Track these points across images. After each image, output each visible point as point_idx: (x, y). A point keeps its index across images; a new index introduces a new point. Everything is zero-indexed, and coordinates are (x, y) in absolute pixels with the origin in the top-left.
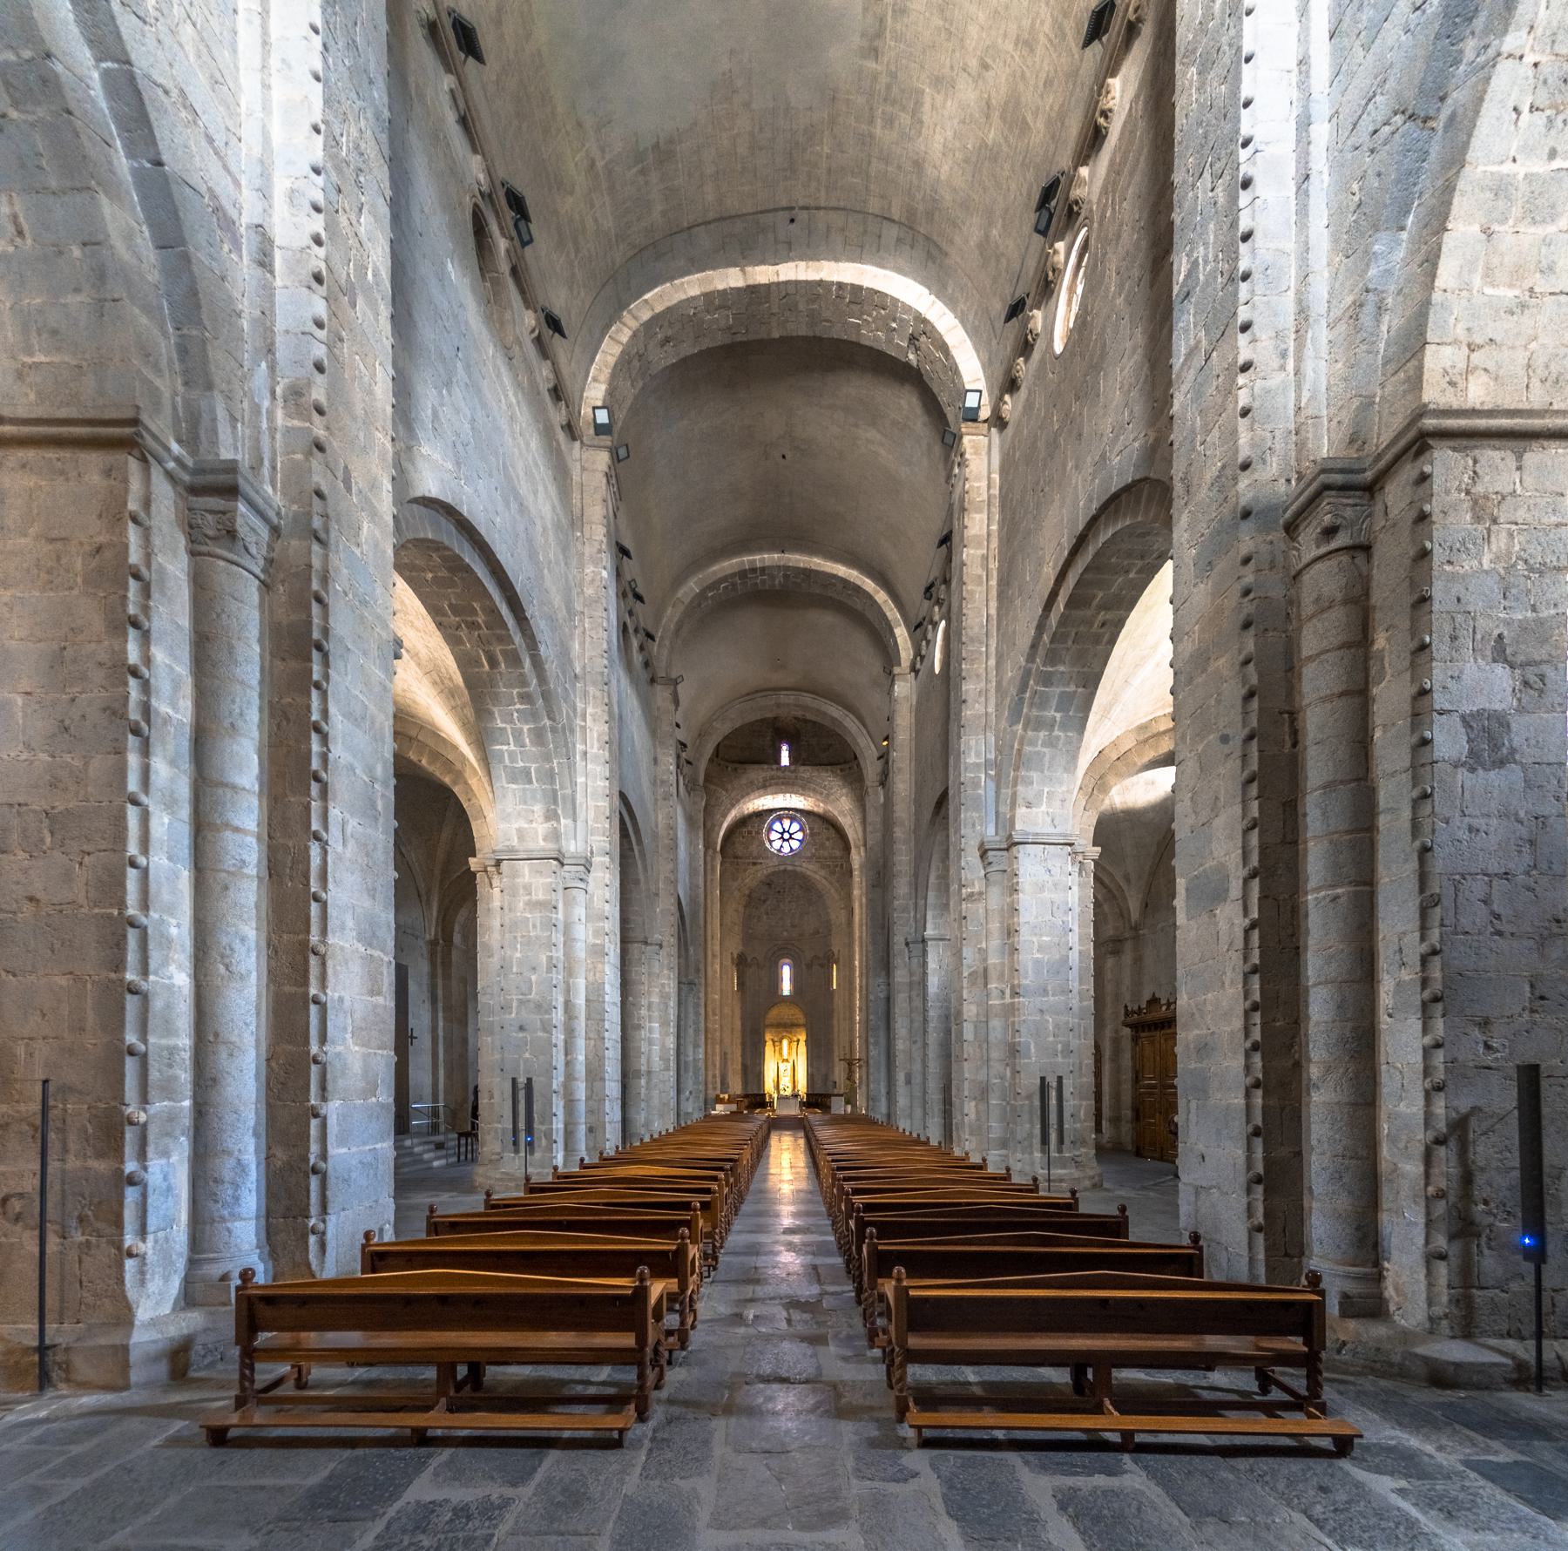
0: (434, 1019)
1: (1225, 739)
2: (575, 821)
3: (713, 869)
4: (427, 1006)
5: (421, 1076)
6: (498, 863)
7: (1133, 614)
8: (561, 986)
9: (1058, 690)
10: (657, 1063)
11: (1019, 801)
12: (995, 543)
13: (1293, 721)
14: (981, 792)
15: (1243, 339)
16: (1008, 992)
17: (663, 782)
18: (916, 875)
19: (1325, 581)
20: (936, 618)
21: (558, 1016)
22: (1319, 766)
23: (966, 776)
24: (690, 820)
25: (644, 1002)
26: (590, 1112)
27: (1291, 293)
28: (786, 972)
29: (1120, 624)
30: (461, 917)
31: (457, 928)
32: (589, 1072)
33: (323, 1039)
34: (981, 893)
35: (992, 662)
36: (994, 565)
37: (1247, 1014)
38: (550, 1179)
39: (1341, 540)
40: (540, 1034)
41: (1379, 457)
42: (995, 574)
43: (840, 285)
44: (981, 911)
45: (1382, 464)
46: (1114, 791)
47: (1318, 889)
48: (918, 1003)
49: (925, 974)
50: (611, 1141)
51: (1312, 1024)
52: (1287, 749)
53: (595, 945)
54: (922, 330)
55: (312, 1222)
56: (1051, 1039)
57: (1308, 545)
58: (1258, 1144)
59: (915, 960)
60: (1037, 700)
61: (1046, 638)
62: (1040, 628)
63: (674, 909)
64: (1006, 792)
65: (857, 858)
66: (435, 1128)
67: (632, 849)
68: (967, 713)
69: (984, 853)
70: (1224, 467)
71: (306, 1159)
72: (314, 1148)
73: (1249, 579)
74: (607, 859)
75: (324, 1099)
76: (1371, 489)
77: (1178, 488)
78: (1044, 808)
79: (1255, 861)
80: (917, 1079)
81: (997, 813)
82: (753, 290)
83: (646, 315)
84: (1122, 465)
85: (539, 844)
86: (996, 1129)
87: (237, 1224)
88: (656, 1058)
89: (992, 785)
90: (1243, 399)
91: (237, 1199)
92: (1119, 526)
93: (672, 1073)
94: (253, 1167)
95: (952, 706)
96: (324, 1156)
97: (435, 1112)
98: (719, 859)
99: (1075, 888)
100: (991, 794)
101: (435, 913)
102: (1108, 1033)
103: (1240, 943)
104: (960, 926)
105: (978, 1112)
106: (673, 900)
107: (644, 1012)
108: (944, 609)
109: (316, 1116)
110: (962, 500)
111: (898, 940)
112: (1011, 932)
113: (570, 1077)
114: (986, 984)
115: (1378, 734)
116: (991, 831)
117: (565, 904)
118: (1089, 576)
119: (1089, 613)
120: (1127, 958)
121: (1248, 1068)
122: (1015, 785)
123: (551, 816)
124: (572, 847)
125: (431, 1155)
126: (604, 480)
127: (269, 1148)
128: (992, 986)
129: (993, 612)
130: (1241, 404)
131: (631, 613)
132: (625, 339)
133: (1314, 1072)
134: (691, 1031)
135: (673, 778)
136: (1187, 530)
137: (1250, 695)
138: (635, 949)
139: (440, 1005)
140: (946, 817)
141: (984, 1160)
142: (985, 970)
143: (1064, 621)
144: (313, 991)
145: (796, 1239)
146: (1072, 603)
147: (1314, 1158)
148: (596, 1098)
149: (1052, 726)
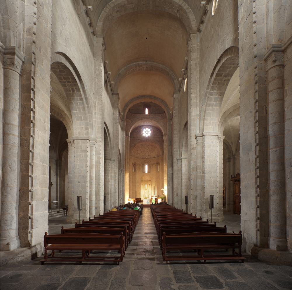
0: (57, 180)
1: (251, 112)
2: (93, 130)
3: (128, 141)
4: (55, 176)
5: (54, 194)
6: (74, 140)
7: (232, 78)
8: (89, 171)
9: (214, 97)
10: (113, 191)
11: (205, 124)
12: (199, 60)
13: (266, 108)
14: (196, 122)
15: (254, 16)
16: (202, 172)
17: (115, 119)
18: (180, 143)
19: (273, 73)
20: (185, 78)
21: (88, 179)
22: (272, 119)
23: (192, 118)
24: (122, 129)
25: (110, 175)
26: (96, 203)
27: (265, 5)
28: (146, 167)
29: (229, 80)
30: (65, 152)
31: (63, 157)
32: (96, 193)
33: (32, 186)
34: (195, 148)
35: (198, 89)
36: (198, 65)
37: (256, 178)
38: (88, 220)
39: (277, 63)
40: (83, 184)
41: (285, 44)
42: (199, 67)
44: (196, 152)
45: (286, 46)
46: (229, 121)
47: (272, 148)
48: (180, 175)
49: (182, 167)
50: (102, 213)
51: (271, 181)
52: (265, 115)
53: (98, 161)
55: (29, 230)
56: (212, 184)
57: (270, 64)
58: (258, 209)
59: (179, 164)
60: (209, 99)
61: (211, 84)
62: (210, 81)
64: (202, 122)
65: (165, 138)
66: (57, 208)
67: (107, 137)
68: (192, 102)
69: (196, 138)
70: (250, 45)
71: (28, 215)
72: (30, 212)
73: (257, 72)
74: (101, 139)
75: (32, 200)
76: (284, 51)
77: (240, 50)
78: (211, 126)
79: (258, 142)
80: (179, 194)
81: (199, 127)
84: (228, 43)
85: (84, 136)
86: (199, 207)
87: (11, 231)
88: (113, 190)
89: (198, 120)
90: (254, 30)
91: (11, 225)
92: (228, 57)
93: (117, 193)
94: (15, 217)
95: (188, 100)
96: (32, 214)
97: (57, 204)
99: (219, 146)
100: (198, 123)
101: (57, 153)
102: (227, 182)
103: (254, 162)
104: (190, 156)
105: (194, 203)
107: (110, 177)
108: (186, 76)
109: (30, 205)
110: (190, 49)
111: (175, 159)
112: (203, 157)
113: (91, 195)
114: (196, 171)
115: (286, 109)
116: (198, 132)
117: (90, 151)
118: (221, 69)
119: (221, 78)
120: (232, 163)
121: (256, 191)
122: (204, 120)
123: (87, 129)
124: (92, 136)
125: (56, 214)
127: (19, 212)
128: (198, 171)
129: (198, 77)
130: (254, 31)
133: (271, 192)
134: (122, 182)
135: (118, 118)
136: (242, 59)
137: (256, 102)
138: (107, 161)
139: (58, 176)
140: (187, 128)
141: (196, 215)
142: (196, 167)
143: (215, 80)
144: (30, 174)
145: (148, 235)
146: (217, 75)
147: (271, 213)
148: (97, 200)
149: (213, 105)
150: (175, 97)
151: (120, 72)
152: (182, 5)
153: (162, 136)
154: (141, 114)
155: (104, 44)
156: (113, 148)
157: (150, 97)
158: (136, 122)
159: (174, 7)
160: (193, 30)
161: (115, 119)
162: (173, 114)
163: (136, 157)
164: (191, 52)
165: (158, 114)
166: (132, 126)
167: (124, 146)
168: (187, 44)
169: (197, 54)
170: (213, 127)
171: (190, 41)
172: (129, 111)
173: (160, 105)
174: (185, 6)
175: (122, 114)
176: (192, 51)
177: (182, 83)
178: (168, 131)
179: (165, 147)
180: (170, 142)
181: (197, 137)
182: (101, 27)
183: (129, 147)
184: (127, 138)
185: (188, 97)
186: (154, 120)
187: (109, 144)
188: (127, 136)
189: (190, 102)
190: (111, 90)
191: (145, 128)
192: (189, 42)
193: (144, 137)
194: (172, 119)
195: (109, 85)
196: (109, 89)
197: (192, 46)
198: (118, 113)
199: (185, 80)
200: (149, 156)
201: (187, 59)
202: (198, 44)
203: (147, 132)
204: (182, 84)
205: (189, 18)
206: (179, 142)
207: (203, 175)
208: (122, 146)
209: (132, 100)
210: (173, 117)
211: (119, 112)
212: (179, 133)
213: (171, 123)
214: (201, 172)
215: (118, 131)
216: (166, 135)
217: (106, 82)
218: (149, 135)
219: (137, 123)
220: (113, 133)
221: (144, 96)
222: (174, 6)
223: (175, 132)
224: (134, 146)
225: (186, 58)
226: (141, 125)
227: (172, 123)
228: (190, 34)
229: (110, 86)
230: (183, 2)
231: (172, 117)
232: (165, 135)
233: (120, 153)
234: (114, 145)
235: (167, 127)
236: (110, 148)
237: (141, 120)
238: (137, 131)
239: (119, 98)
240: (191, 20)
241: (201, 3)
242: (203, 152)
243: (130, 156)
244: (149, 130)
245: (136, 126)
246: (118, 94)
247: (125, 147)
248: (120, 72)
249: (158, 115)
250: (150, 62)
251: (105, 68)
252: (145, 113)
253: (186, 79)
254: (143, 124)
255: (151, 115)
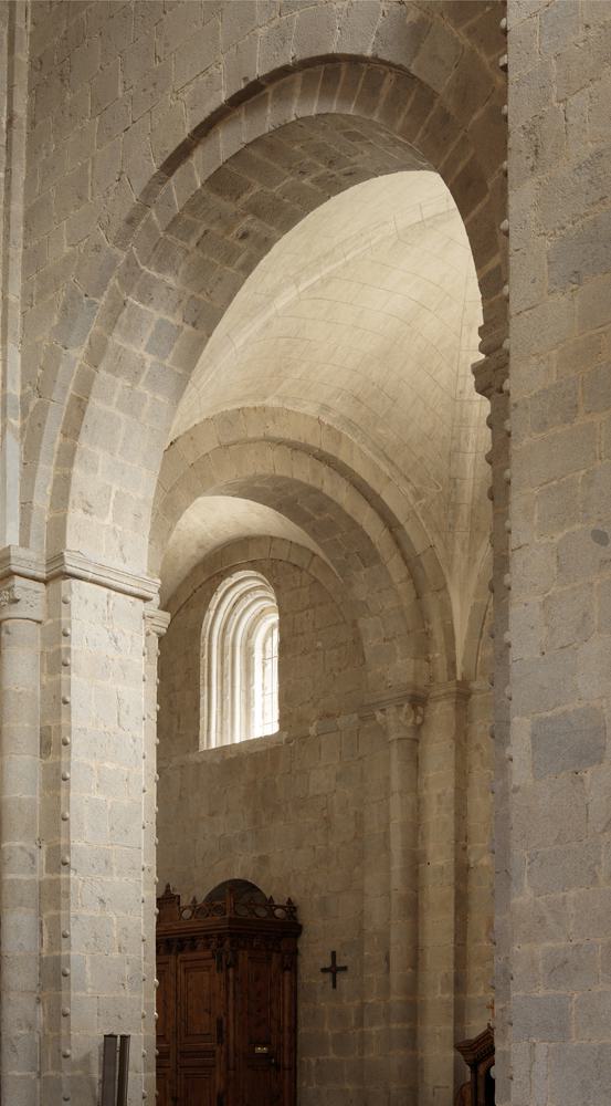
16: (42, 857)
64: (46, 470)
78: (108, 520)
170: (120, 528)
181: (11, 574)
207: (55, 884)
214: (33, 857)
242: (57, 701)
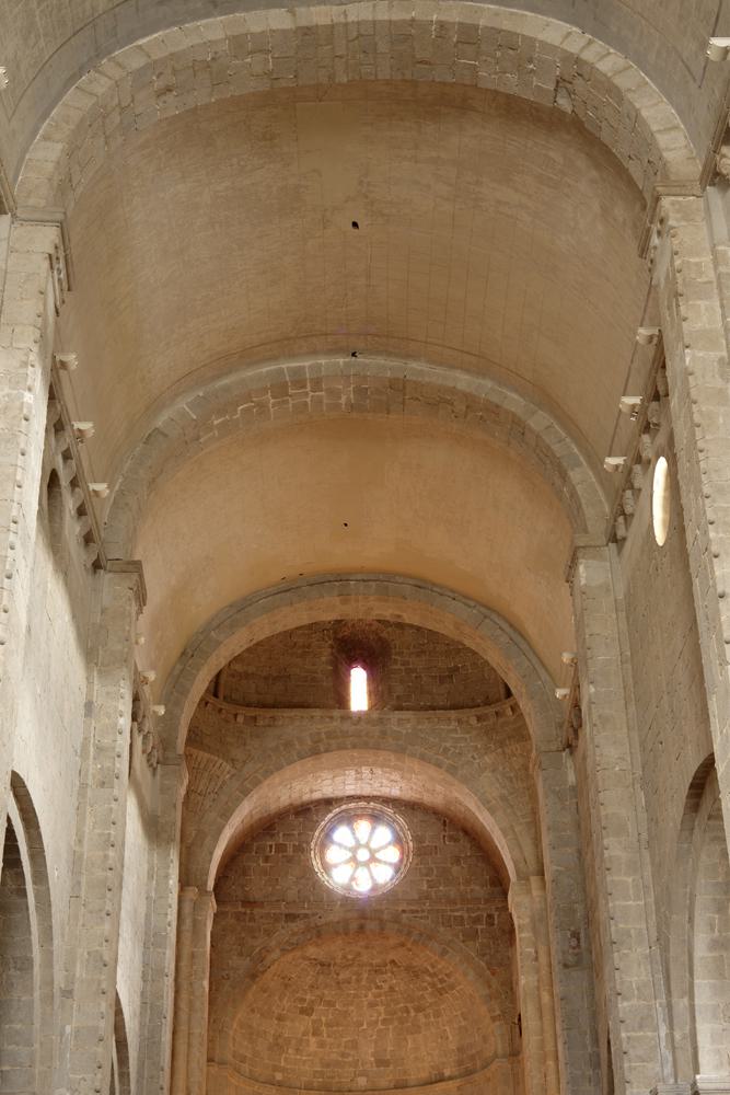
17: (100, 749)
18: (662, 941)
20: (647, 454)
24: (154, 828)
43: (442, 25)
54: (574, 73)
63: (106, 1026)
65: (522, 905)
67: (23, 893)
82: (307, 31)
83: (137, 63)
98: (211, 907)
106: (105, 1006)
108: (661, 439)
126: (46, 264)
131: (67, 456)
132: (100, 90)
135: (123, 743)
150: (583, 582)
151: (160, 422)
152: (588, 56)
153: (499, 883)
154: (317, 713)
155: (65, 260)
156: (68, 993)
157: (383, 581)
158: (268, 773)
159: (531, 66)
160: (673, 178)
161: (100, 749)
162: (577, 706)
163: (272, 1082)
164: (677, 295)
165: (455, 707)
166: (238, 801)
167: (161, 973)
168: (644, 250)
169: (722, 306)
171: (659, 233)
172: (215, 688)
173: (467, 643)
174: (607, 61)
175: (161, 710)
176: (680, 289)
177: (629, 484)
178: (546, 840)
179: (525, 981)
180: (576, 935)
182: (50, 167)
183: (206, 983)
184: (187, 908)
185: (696, 582)
186: (423, 758)
187: (30, 961)
188: (192, 893)
189: (717, 612)
190: (88, 539)
191: (349, 819)
192: (655, 240)
193: (349, 902)
194: (570, 747)
195: (70, 503)
196: (72, 529)
197: (678, 263)
198: (126, 706)
199: (648, 465)
200: (381, 1062)
201: (651, 338)
202: (720, 248)
203: (363, 855)
204: (629, 493)
205: (637, 112)
206: (654, 935)
208: (144, 978)
209: (240, 610)
210: (587, 728)
211: (136, 699)
212: (646, 854)
213: (571, 778)
215: (115, 844)
216: (534, 880)
217: (52, 482)
218: (384, 875)
219: (276, 778)
220: (76, 863)
221: (337, 580)
222: (530, 61)
223: (614, 849)
224: (253, 976)
225: (643, 332)
226: (317, 795)
227: (583, 775)
228: (657, 199)
229: (81, 512)
230: (590, 42)
231: (576, 727)
232: (523, 877)
233: (121, 1044)
234: (79, 971)
235: (534, 812)
236: (37, 994)
237: (315, 752)
238: (281, 848)
239: (141, 598)
240: (654, 128)
241: (705, 45)
243: (214, 1069)
244: (384, 834)
245: (273, 807)
246: (136, 567)
247: (170, 981)
248: (160, 421)
249: (453, 714)
250: (381, 360)
251: (53, 396)
252: (342, 700)
253: (662, 465)
254: (326, 784)
255: (398, 715)
